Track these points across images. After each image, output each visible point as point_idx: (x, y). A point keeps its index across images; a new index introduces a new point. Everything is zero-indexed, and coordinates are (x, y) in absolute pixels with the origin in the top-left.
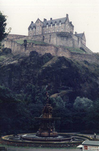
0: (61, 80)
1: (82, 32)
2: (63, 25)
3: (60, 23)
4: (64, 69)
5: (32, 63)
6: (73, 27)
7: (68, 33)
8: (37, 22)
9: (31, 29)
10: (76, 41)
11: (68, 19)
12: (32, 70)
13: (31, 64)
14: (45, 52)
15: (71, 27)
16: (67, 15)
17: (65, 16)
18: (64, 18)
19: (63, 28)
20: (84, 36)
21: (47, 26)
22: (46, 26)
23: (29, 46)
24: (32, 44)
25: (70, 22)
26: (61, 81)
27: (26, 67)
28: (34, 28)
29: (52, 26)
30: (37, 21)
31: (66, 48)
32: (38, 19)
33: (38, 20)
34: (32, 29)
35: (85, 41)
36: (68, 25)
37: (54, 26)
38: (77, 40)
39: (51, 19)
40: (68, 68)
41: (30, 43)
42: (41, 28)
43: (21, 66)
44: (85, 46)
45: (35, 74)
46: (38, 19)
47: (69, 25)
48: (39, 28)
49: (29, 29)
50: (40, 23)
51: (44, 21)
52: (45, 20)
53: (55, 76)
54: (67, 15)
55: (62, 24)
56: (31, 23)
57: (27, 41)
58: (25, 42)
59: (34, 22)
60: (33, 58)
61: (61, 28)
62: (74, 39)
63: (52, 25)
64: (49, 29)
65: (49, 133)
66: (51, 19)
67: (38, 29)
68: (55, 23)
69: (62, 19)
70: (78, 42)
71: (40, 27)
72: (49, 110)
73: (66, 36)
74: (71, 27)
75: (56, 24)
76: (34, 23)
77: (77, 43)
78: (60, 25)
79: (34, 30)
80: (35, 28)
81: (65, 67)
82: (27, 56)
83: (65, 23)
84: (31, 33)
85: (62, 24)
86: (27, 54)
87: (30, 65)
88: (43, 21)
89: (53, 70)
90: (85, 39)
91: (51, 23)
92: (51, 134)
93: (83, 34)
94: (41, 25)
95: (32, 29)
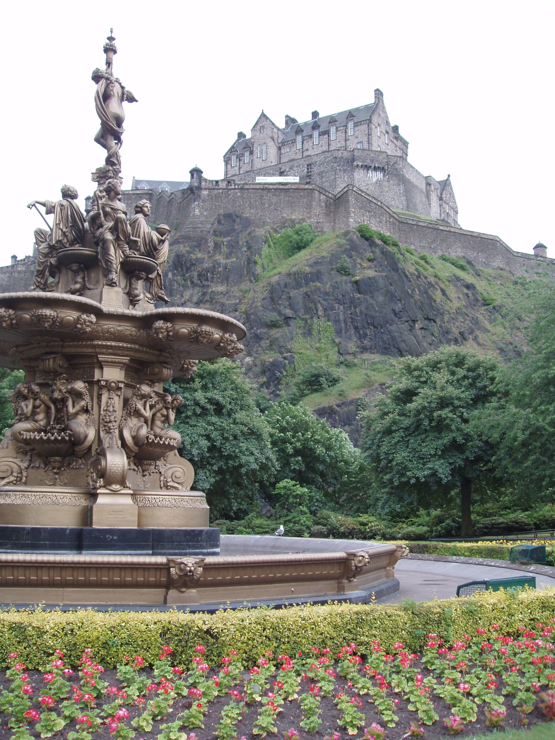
0: (356, 328)
1: (446, 178)
2: (364, 127)
3: (351, 125)
4: (370, 278)
5: (222, 261)
6: (405, 144)
7: (385, 155)
8: (258, 127)
9: (234, 158)
10: (421, 191)
11: (384, 108)
12: (221, 288)
13: (219, 264)
14: (285, 215)
15: (399, 143)
16: (378, 94)
17: (371, 100)
18: (367, 107)
19: (362, 142)
20: (452, 194)
21: (299, 138)
22: (294, 141)
23: (216, 191)
24: (227, 185)
25: (392, 125)
26: (353, 331)
27: (196, 276)
28: (247, 154)
29: (320, 135)
30: (257, 123)
31: (375, 199)
32: (263, 116)
33: (260, 118)
34: (240, 158)
35: (457, 213)
36: (384, 132)
37: (326, 136)
38: (425, 190)
39: (315, 114)
40: (386, 276)
41: (217, 182)
42: (273, 151)
43: (174, 274)
44: (455, 222)
45: (236, 304)
46: (263, 113)
47: (387, 132)
48: (264, 148)
49: (227, 160)
50: (268, 132)
51: (287, 123)
52: (290, 121)
53: (325, 310)
54: (378, 94)
55: (356, 125)
56: (236, 138)
57: (202, 172)
58: (195, 176)
59: (249, 136)
60: (229, 238)
61: (356, 141)
62: (409, 182)
63: (316, 133)
64: (307, 150)
65: (93, 496)
66: (315, 114)
67: (262, 153)
68: (329, 123)
69: (357, 110)
70: (428, 197)
71: (271, 144)
72: (109, 236)
73: (377, 165)
74: (395, 141)
75: (333, 130)
76: (247, 138)
77: (424, 199)
78: (350, 132)
79: (247, 158)
80: (251, 153)
81: (371, 273)
82: (202, 231)
83: (370, 121)
84: (234, 173)
85: (356, 125)
86: (200, 225)
87: (212, 270)
88: (281, 124)
89: (319, 284)
90: (455, 202)
91: (315, 126)
92: (101, 500)
93: (445, 184)
94: (276, 137)
95: (240, 158)
